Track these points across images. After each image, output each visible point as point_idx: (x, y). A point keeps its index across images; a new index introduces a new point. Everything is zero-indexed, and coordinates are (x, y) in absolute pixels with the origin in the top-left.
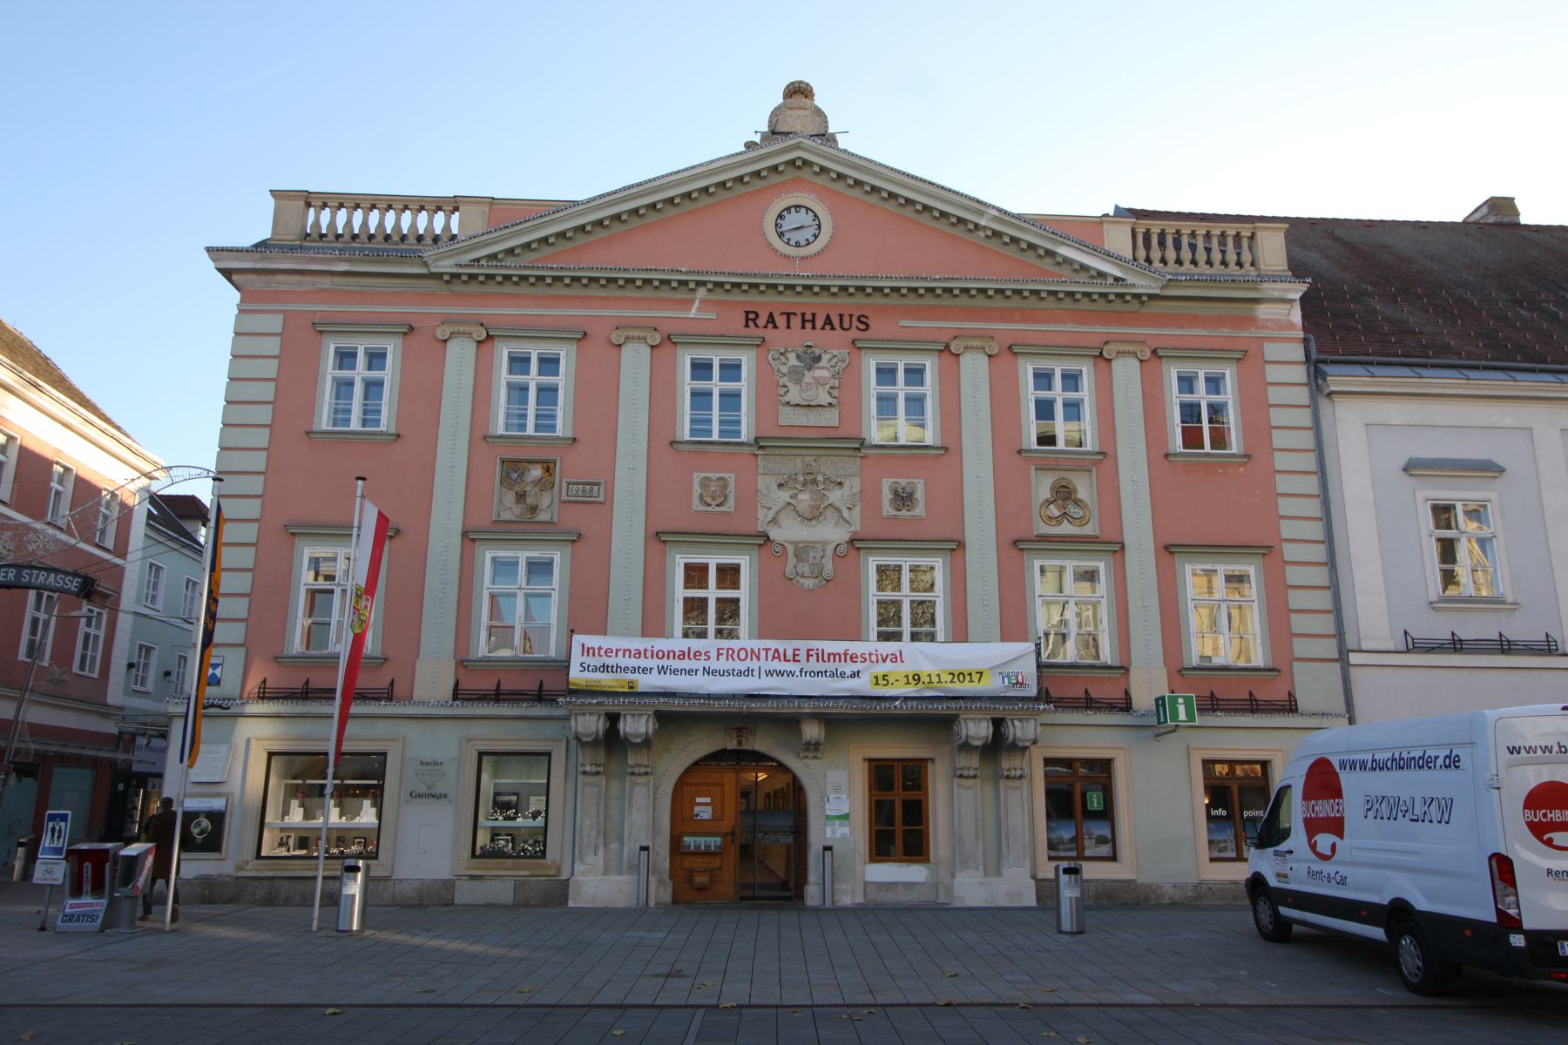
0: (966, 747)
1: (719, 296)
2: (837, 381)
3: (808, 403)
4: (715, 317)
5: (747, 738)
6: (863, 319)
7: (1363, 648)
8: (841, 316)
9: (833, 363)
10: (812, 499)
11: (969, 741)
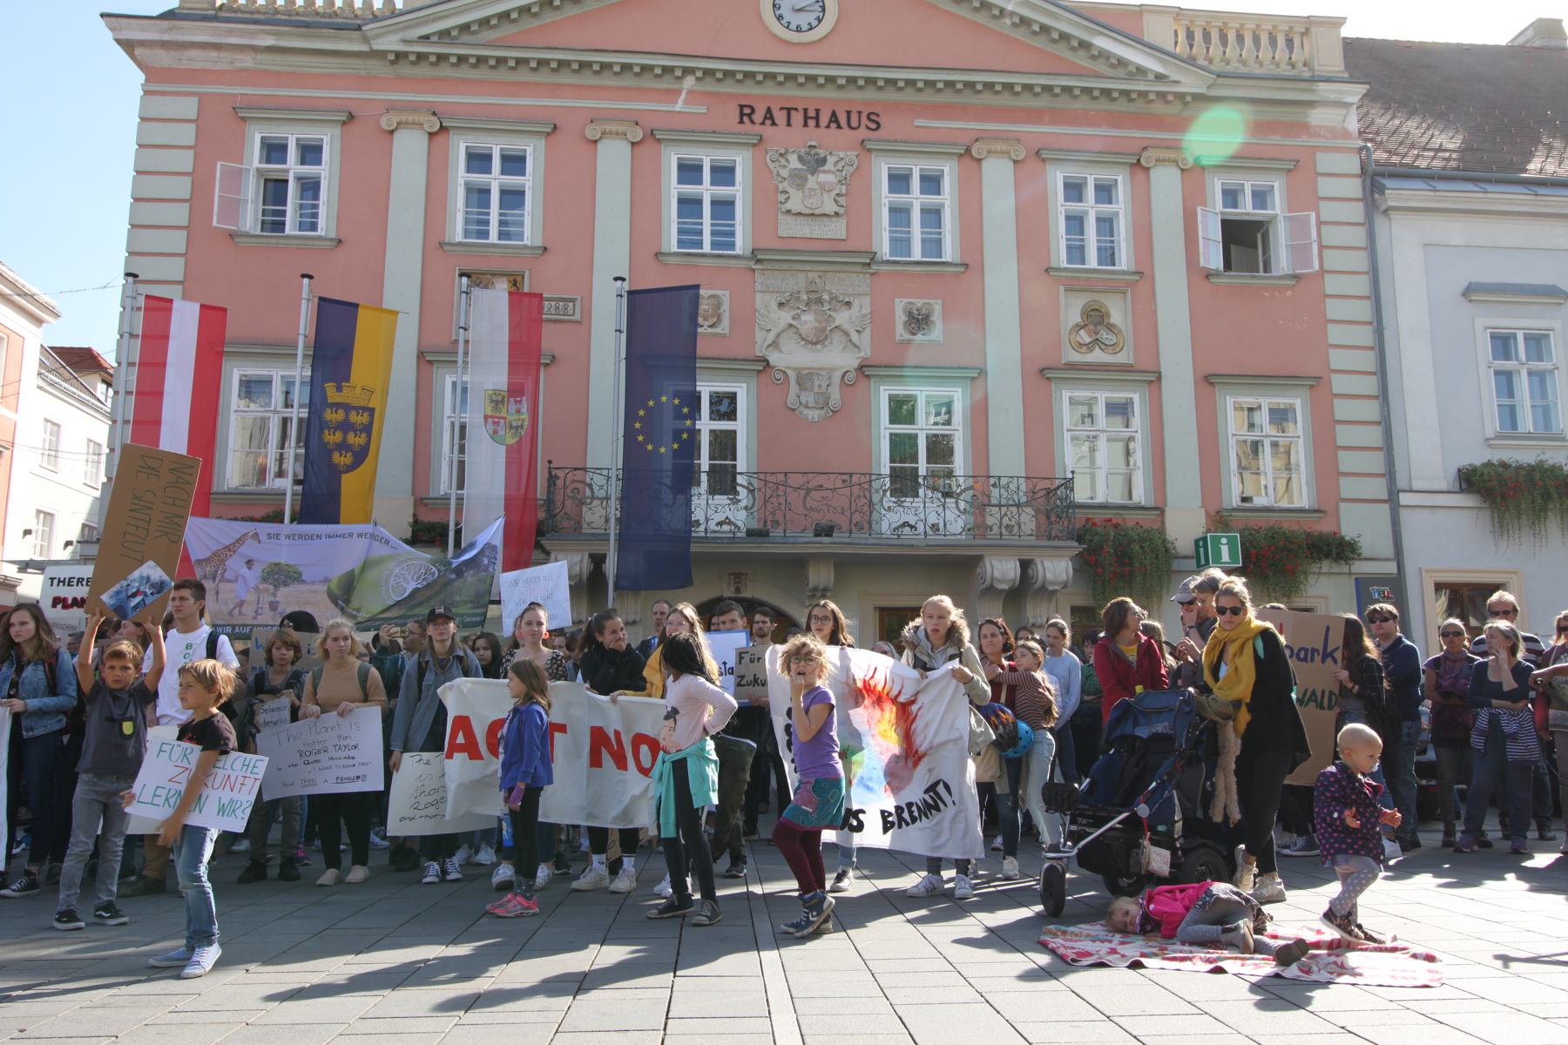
0: (990, 591)
1: (710, 86)
2: (844, 188)
3: (811, 212)
5: (746, 586)
6: (873, 117)
7: (1414, 488)
8: (849, 113)
9: (840, 166)
10: (817, 321)
11: (995, 584)
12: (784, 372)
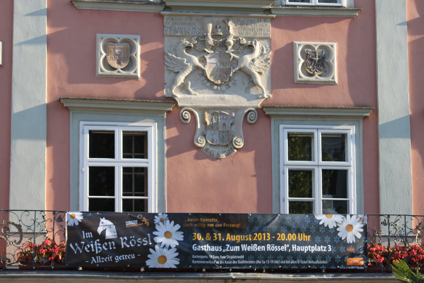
12: (192, 113)
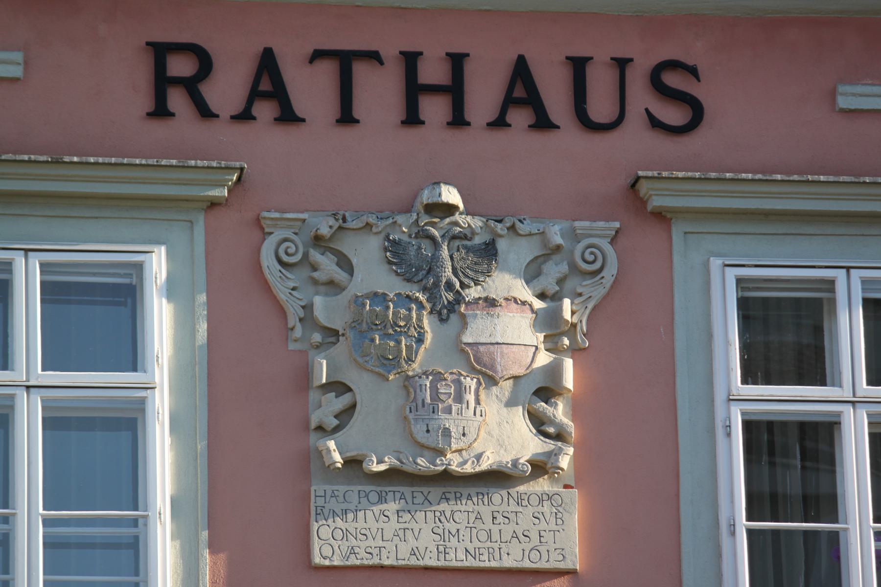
4: (17, 71)
6: (672, 80)
